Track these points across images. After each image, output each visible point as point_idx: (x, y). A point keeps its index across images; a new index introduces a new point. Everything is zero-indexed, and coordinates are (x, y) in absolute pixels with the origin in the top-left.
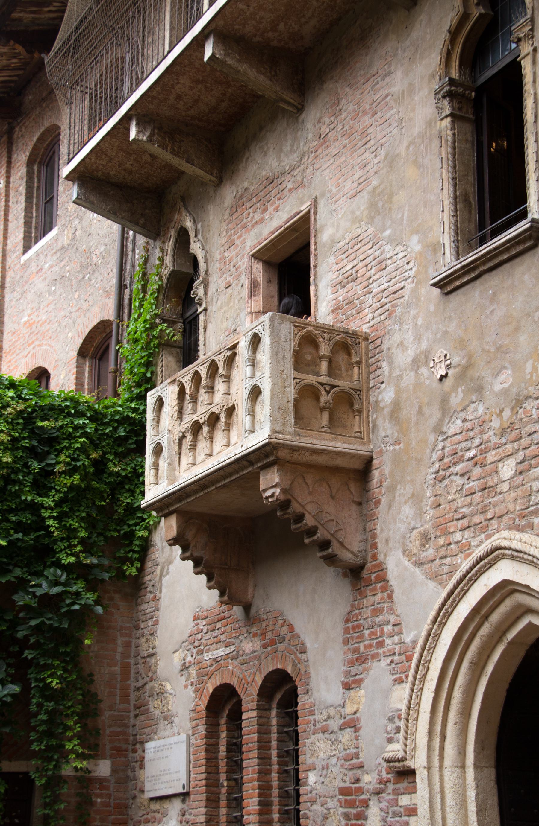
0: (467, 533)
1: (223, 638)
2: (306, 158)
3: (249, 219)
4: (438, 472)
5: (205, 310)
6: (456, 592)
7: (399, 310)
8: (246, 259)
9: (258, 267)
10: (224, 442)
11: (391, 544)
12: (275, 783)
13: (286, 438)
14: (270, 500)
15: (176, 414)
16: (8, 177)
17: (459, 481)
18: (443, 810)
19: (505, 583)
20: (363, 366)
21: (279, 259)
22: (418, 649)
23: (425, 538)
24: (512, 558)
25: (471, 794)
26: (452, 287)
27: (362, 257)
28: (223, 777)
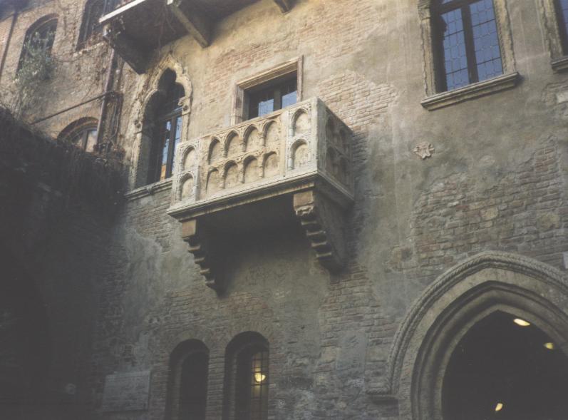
0: (448, 252)
2: (292, 35)
3: (235, 65)
4: (421, 213)
5: (190, 113)
6: (443, 287)
10: (261, 174)
13: (324, 174)
14: (304, 213)
15: (206, 158)
17: (444, 219)
26: (439, 106)
27: (346, 89)
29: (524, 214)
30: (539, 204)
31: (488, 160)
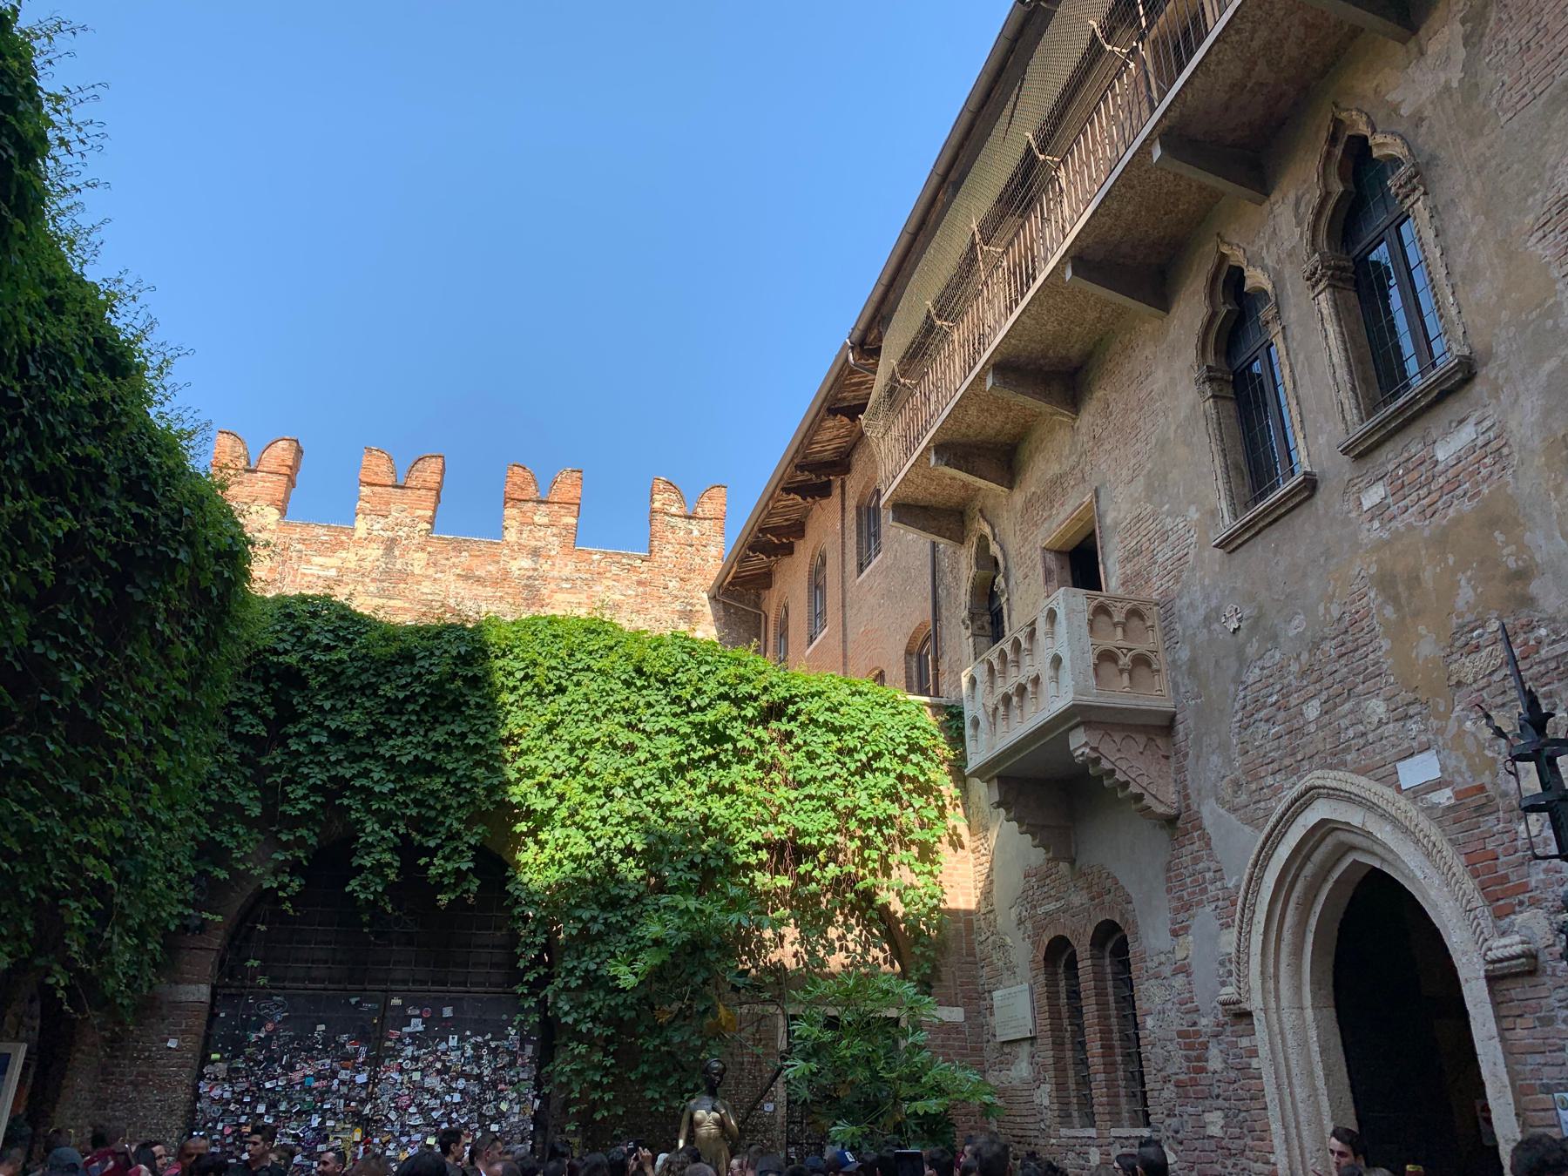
0: (1278, 777)
1: (1053, 893)
4: (1241, 720)
7: (1185, 574)
8: (1039, 551)
9: (1050, 557)
11: (1203, 793)
12: (1115, 1028)
13: (1088, 700)
16: (843, 520)
17: (1263, 727)
18: (1285, 1052)
19: (1323, 822)
20: (1157, 628)
21: (1070, 549)
22: (1242, 892)
23: (1237, 785)
24: (1329, 796)
25: (1313, 1034)
28: (1066, 1022)
29: (1347, 706)
30: (1361, 687)
31: (1298, 625)
